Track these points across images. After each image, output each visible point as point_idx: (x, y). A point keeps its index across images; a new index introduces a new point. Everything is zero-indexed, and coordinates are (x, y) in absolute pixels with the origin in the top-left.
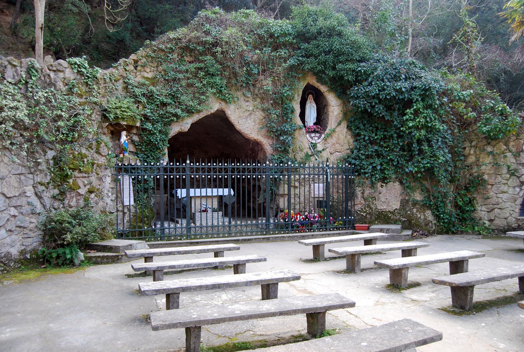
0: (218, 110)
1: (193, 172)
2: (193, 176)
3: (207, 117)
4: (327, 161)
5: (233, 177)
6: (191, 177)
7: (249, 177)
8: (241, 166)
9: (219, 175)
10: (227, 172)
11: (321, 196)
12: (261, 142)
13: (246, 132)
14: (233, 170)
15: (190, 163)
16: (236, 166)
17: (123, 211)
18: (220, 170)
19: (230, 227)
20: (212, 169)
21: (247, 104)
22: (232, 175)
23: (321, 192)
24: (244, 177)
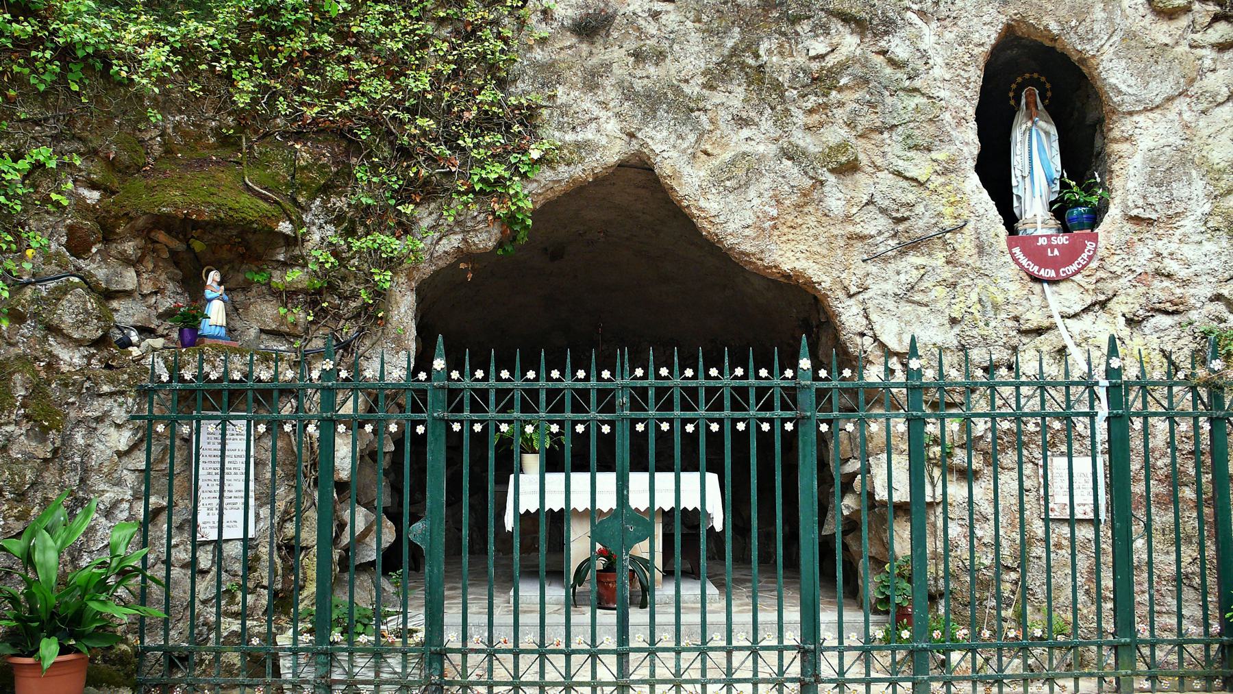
0: (621, 165)
1: (459, 409)
2: (456, 427)
3: (578, 190)
4: (1113, 351)
5: (640, 427)
6: (449, 428)
7: (715, 427)
8: (677, 381)
9: (575, 423)
10: (610, 408)
11: (1084, 510)
12: (810, 283)
13: (747, 247)
14: (639, 398)
15: (449, 368)
16: (652, 381)
17: (192, 564)
18: (580, 400)
19: (622, 656)
20: (543, 396)
21: (746, 132)
22: (634, 422)
23: (1084, 497)
24: (690, 428)
